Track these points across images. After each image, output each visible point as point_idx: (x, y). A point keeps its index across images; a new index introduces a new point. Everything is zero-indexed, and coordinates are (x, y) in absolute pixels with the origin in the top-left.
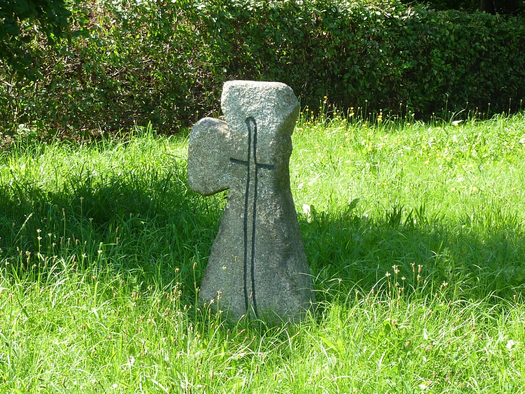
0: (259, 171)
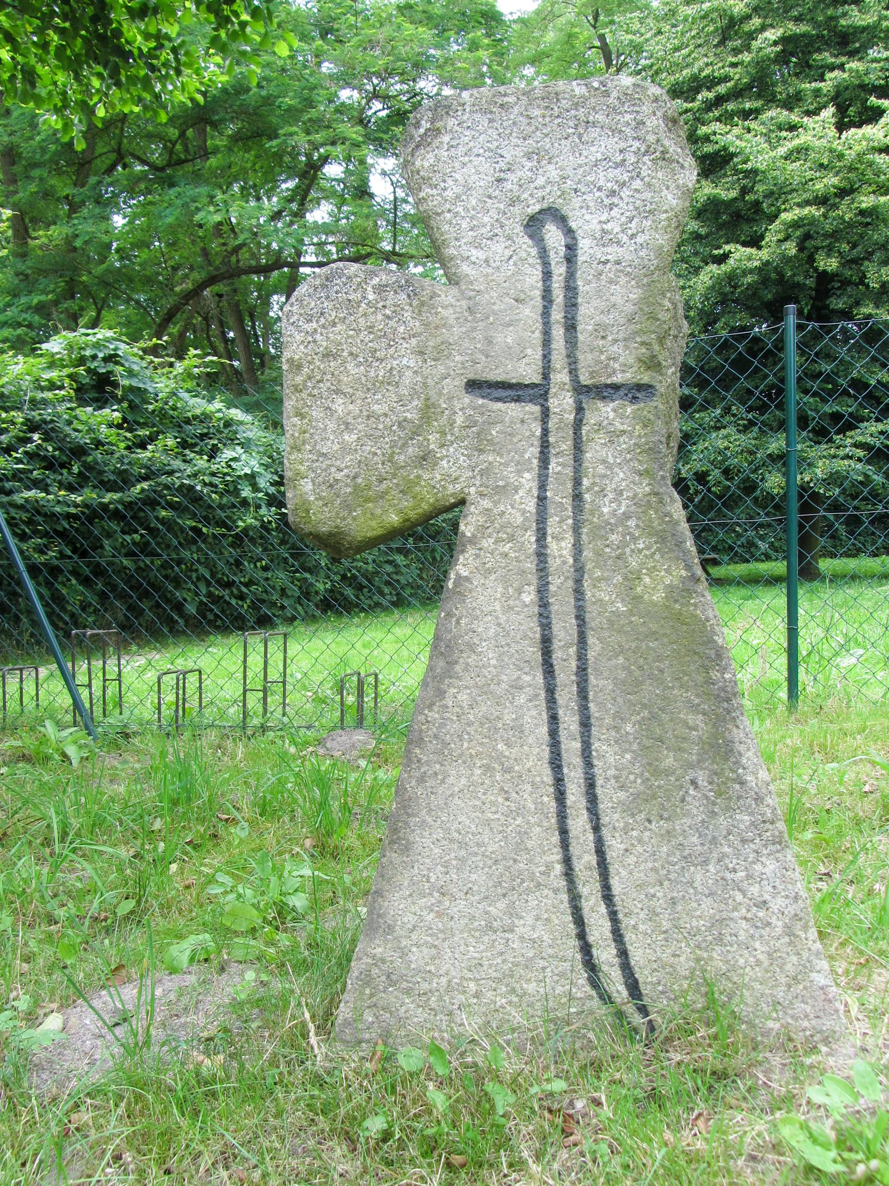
0: (591, 418)
